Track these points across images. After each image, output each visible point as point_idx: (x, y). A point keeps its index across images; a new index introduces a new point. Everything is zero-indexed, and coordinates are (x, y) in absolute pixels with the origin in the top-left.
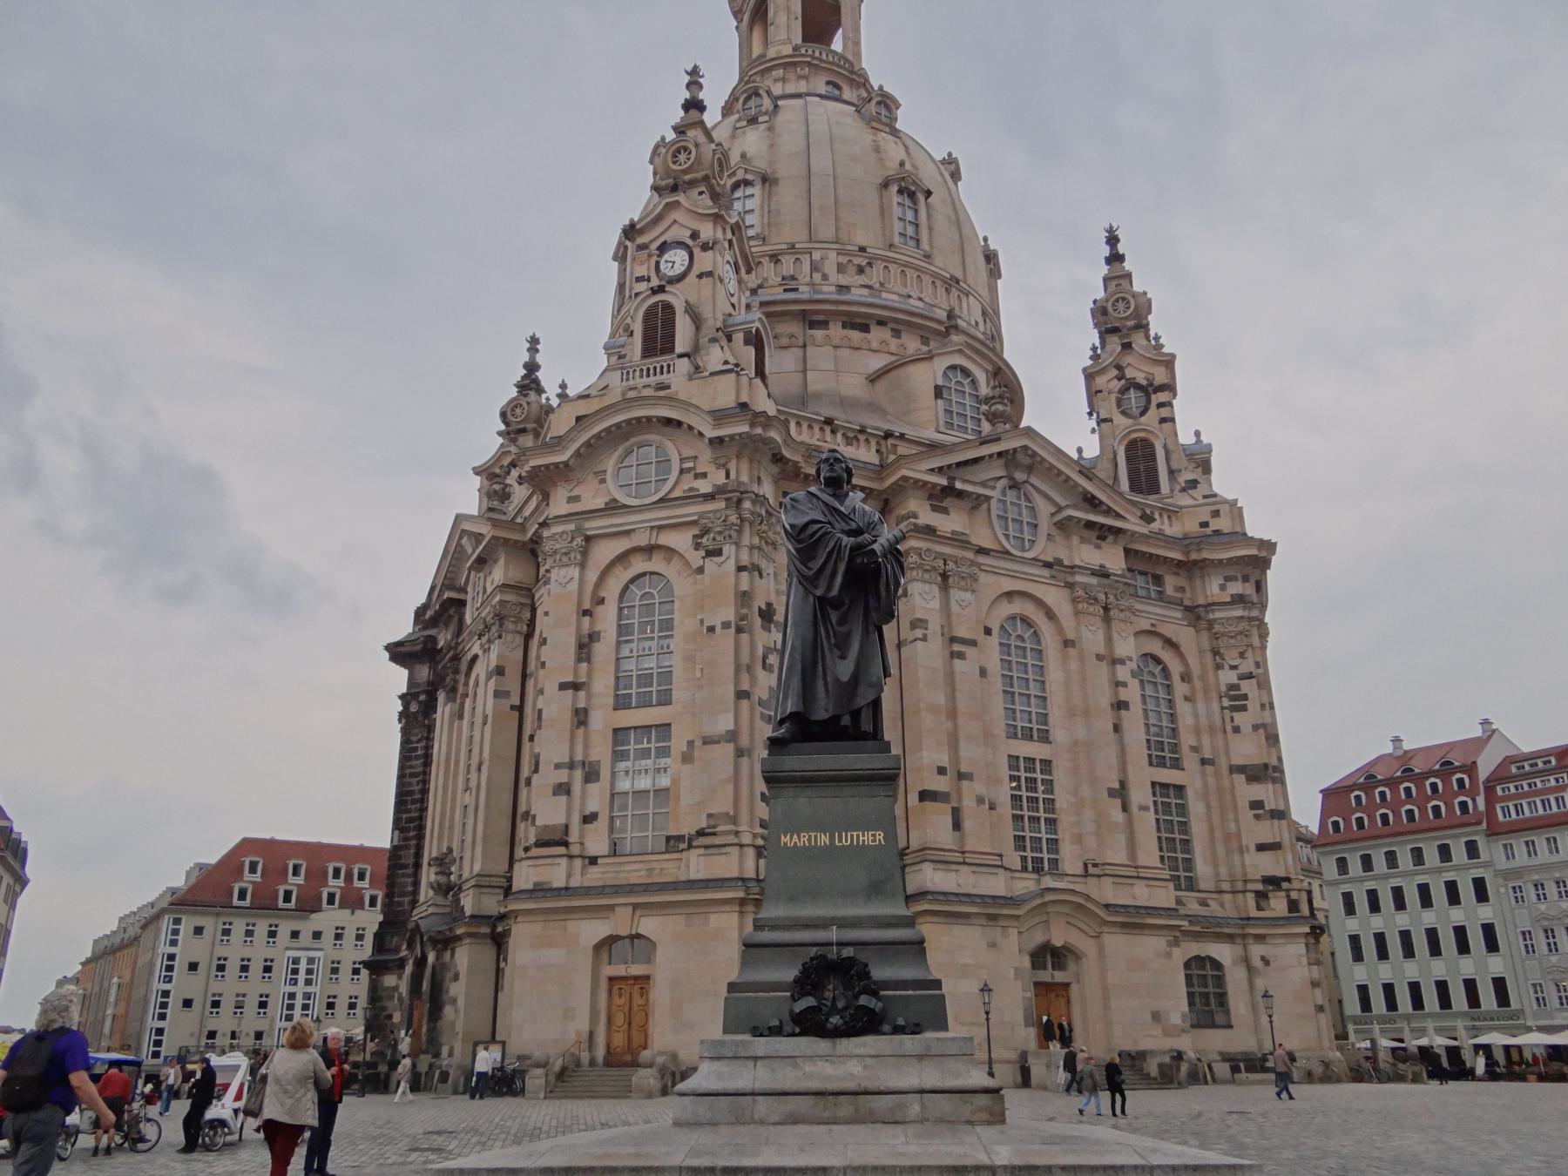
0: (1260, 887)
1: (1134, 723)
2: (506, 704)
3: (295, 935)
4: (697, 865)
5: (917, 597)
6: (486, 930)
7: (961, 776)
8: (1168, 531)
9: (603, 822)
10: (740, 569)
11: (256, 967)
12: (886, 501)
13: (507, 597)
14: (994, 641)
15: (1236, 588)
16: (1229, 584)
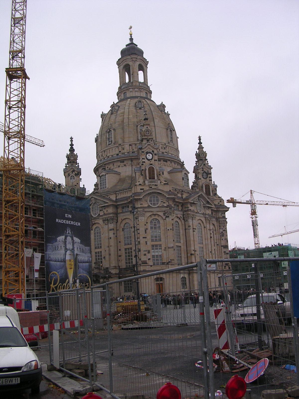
0: (225, 265)
6: (118, 276)
10: (172, 220)
12: (183, 204)
13: (113, 215)
15: (223, 215)
16: (222, 214)
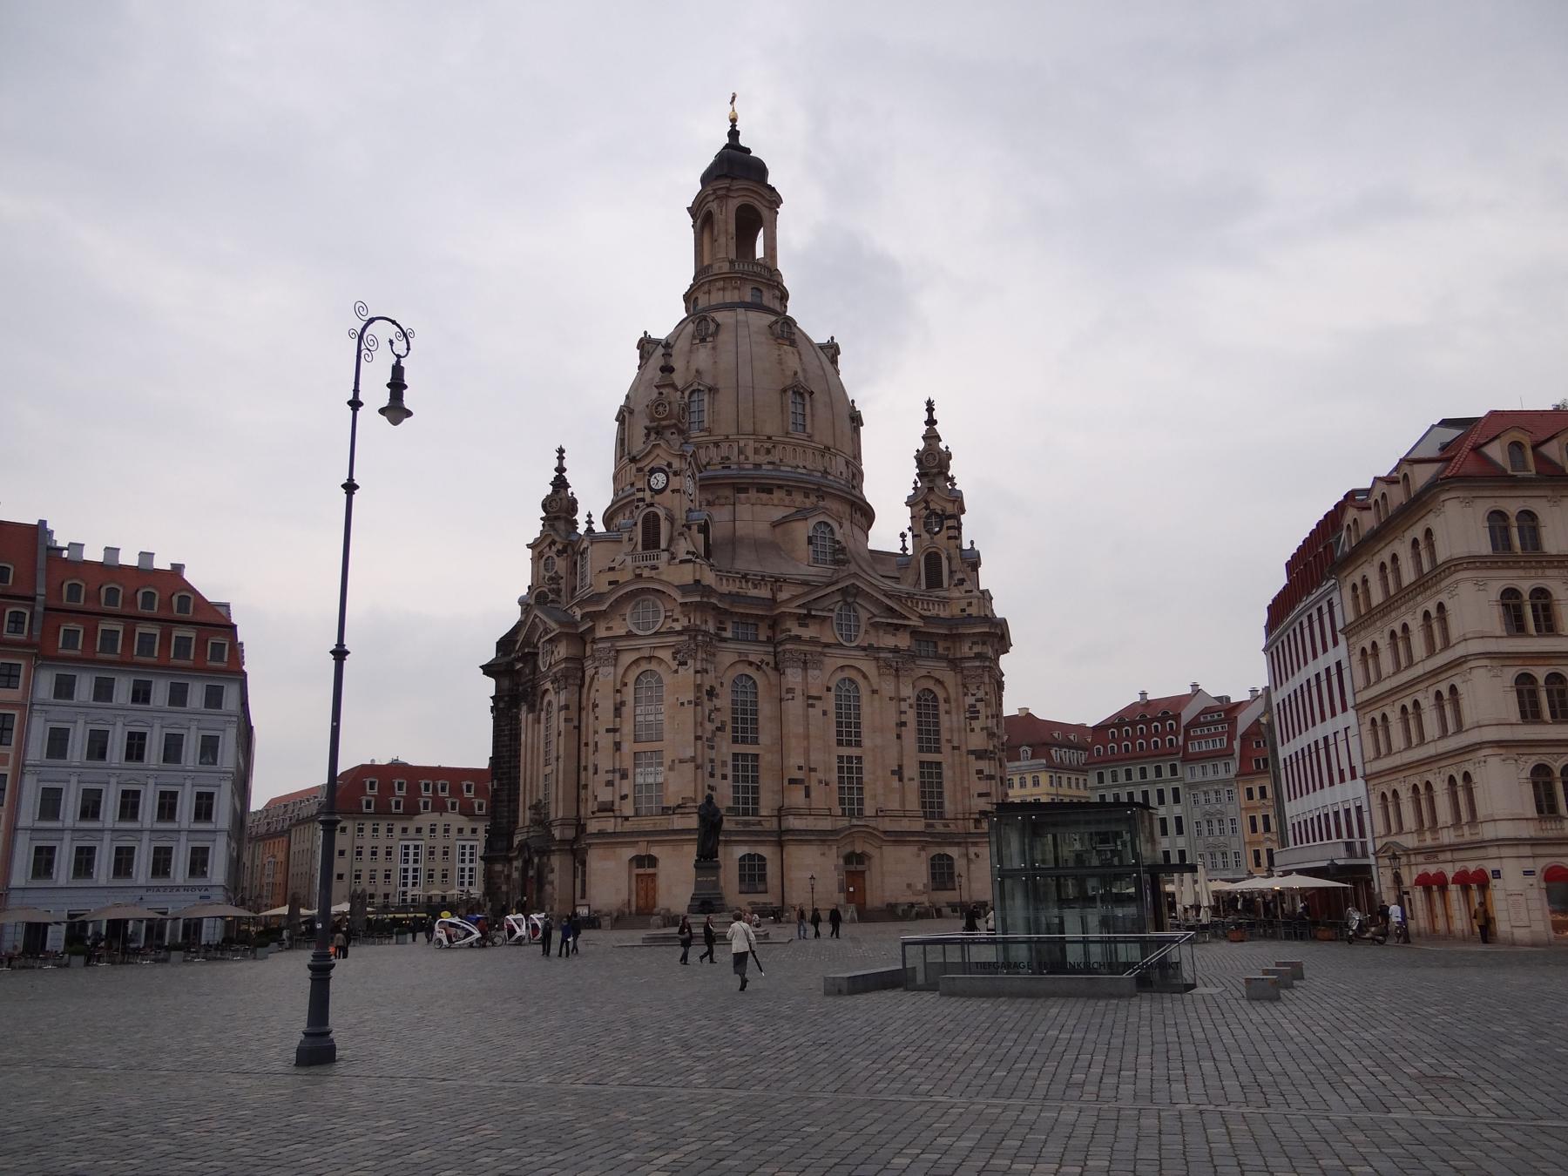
1: (910, 735)
2: (571, 725)
3: (405, 830)
4: (678, 822)
5: (790, 678)
7: (812, 770)
8: (942, 615)
9: (630, 799)
11: (381, 853)
14: (832, 694)
15: (976, 649)
